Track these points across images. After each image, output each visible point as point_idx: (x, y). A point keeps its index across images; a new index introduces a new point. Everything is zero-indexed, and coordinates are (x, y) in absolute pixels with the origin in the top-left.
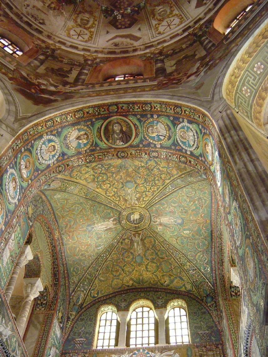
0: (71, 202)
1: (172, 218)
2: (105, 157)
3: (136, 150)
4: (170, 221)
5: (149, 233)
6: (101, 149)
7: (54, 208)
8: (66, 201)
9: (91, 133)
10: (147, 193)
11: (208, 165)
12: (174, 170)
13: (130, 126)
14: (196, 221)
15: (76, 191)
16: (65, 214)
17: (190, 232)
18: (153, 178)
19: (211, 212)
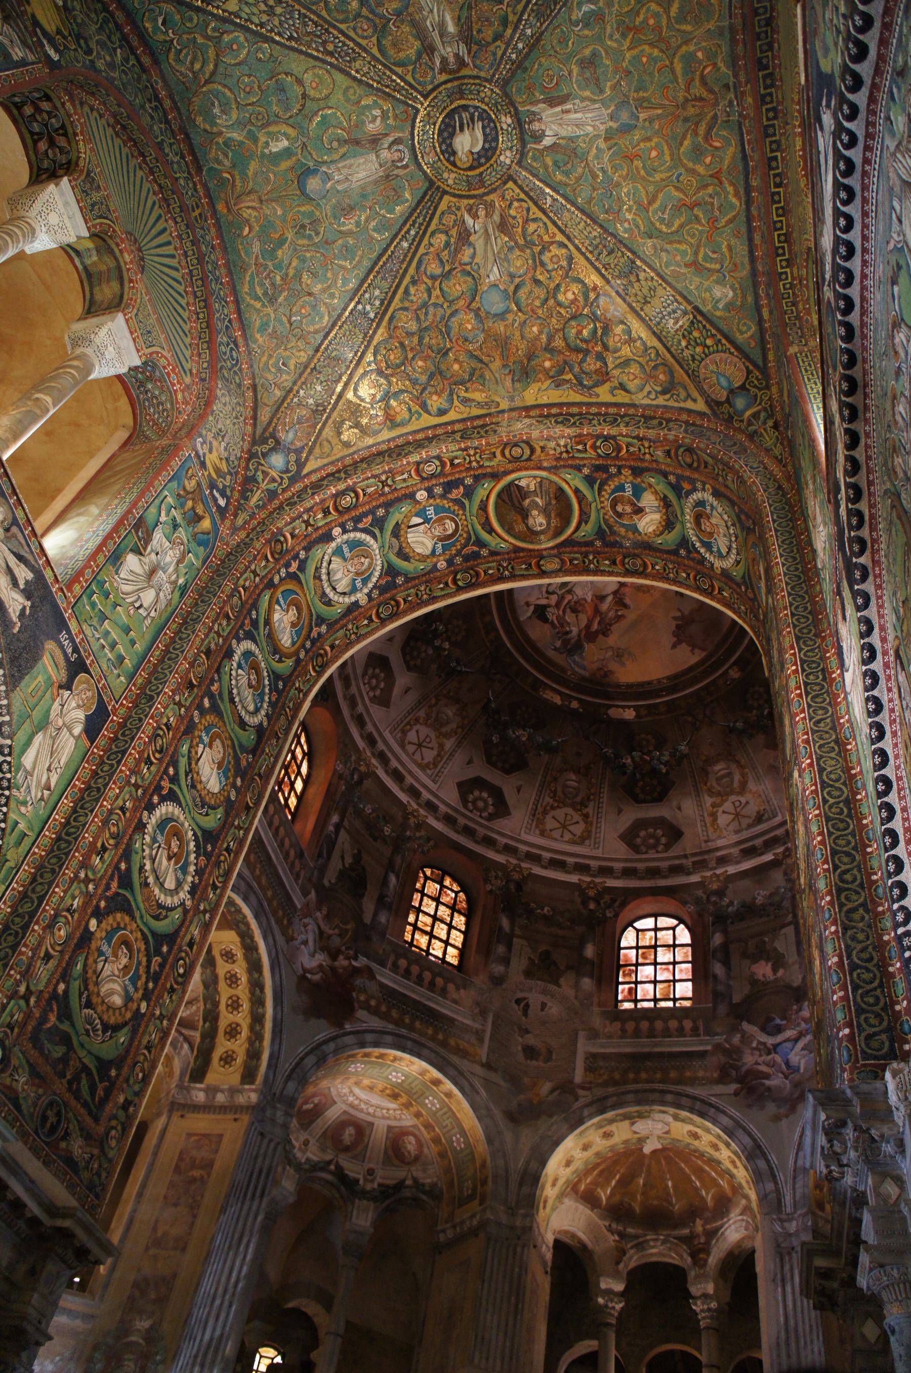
0: (684, 247)
1: (340, 188)
2: (565, 446)
3: (481, 467)
4: (345, 171)
5: (409, 78)
6: (578, 468)
7: (744, 229)
8: (701, 256)
9: (605, 514)
10: (438, 271)
11: (276, 580)
12: (368, 400)
13: (502, 525)
14: (261, 201)
15: (665, 294)
16: (710, 190)
17: (266, 151)
18: (427, 340)
19: (225, 249)
